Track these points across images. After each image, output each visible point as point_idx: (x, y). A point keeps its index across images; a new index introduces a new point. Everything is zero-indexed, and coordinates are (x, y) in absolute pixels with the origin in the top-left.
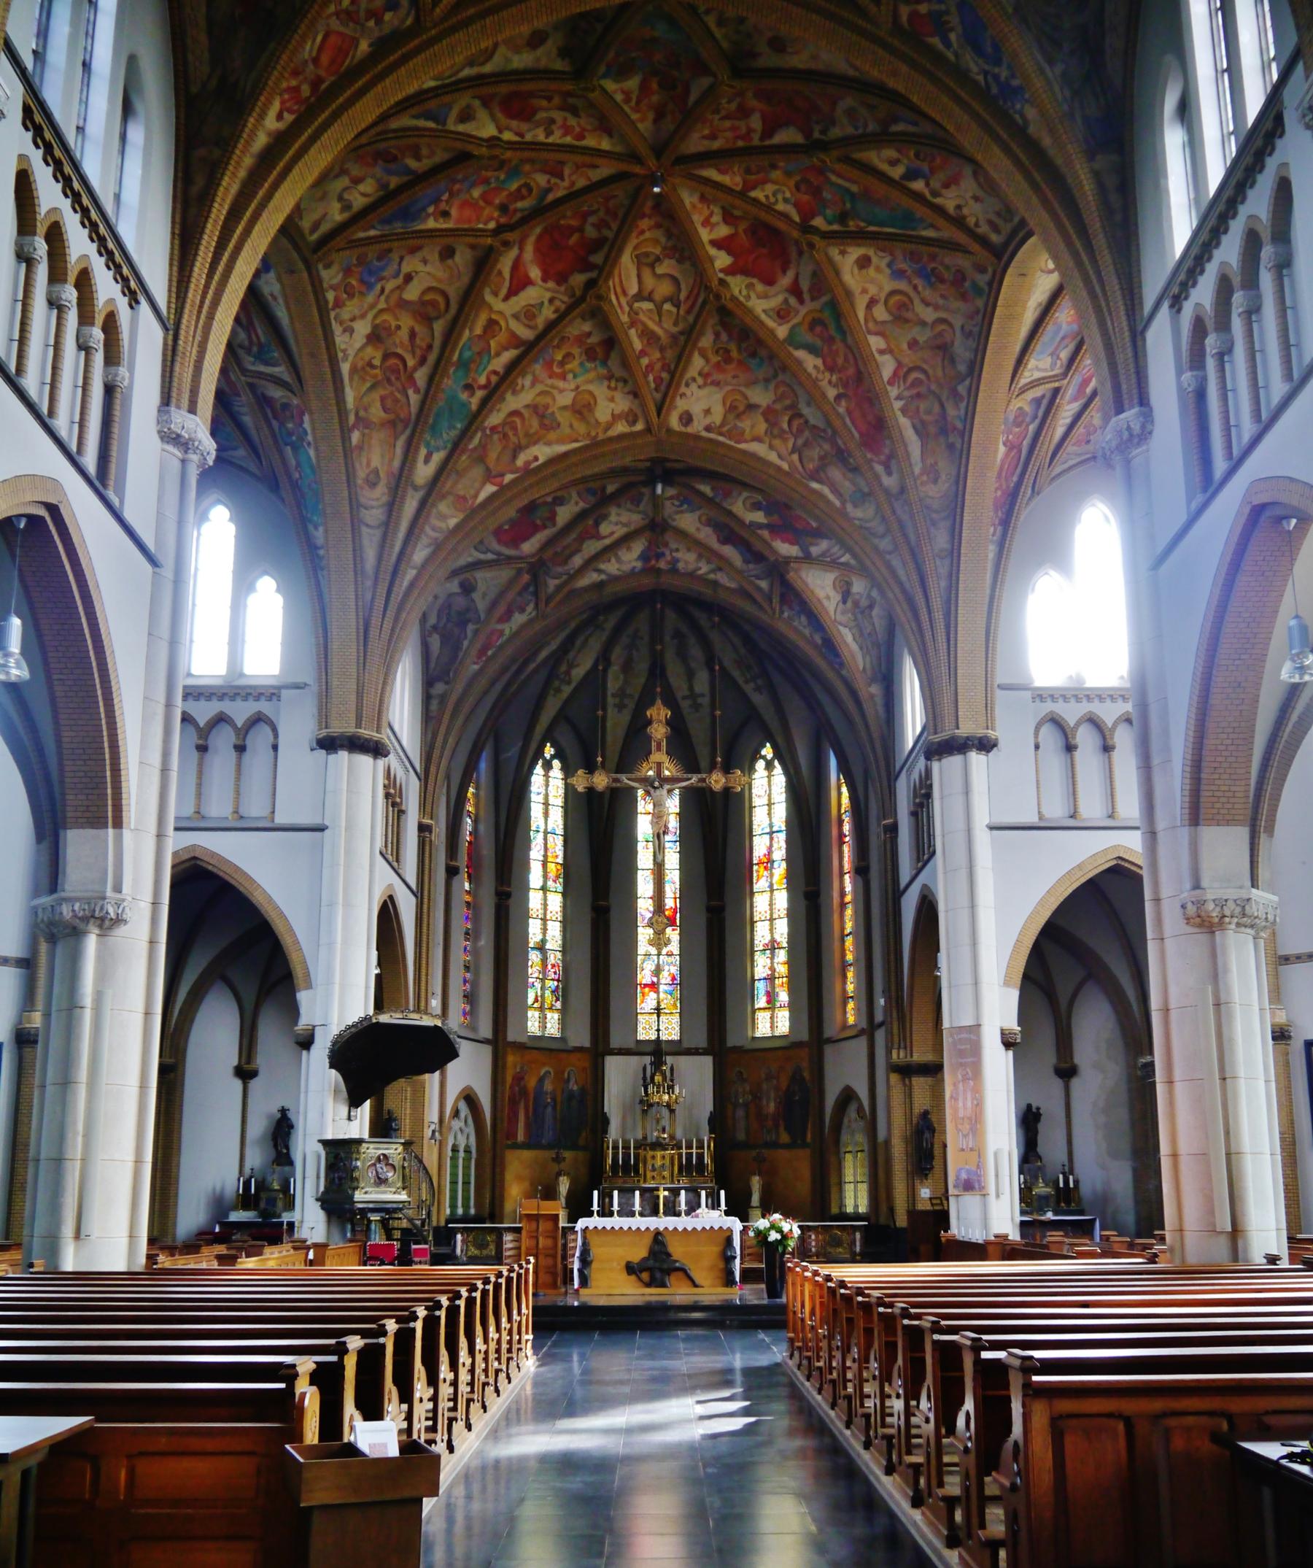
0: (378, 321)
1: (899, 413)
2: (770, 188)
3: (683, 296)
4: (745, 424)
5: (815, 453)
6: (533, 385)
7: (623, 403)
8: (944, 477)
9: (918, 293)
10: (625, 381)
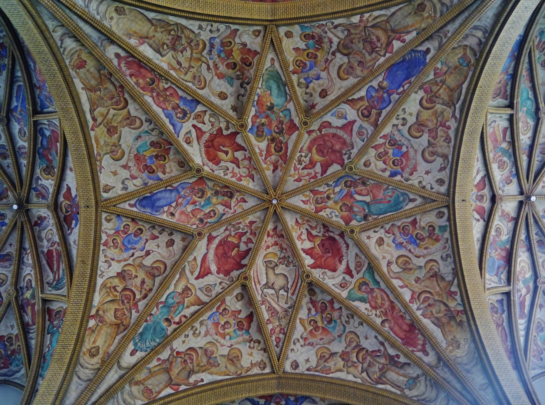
0: (126, 269)
1: (421, 317)
2: (328, 211)
3: (289, 287)
4: (331, 364)
5: (376, 368)
6: (206, 335)
7: (258, 356)
8: (462, 342)
9: (413, 253)
10: (259, 342)
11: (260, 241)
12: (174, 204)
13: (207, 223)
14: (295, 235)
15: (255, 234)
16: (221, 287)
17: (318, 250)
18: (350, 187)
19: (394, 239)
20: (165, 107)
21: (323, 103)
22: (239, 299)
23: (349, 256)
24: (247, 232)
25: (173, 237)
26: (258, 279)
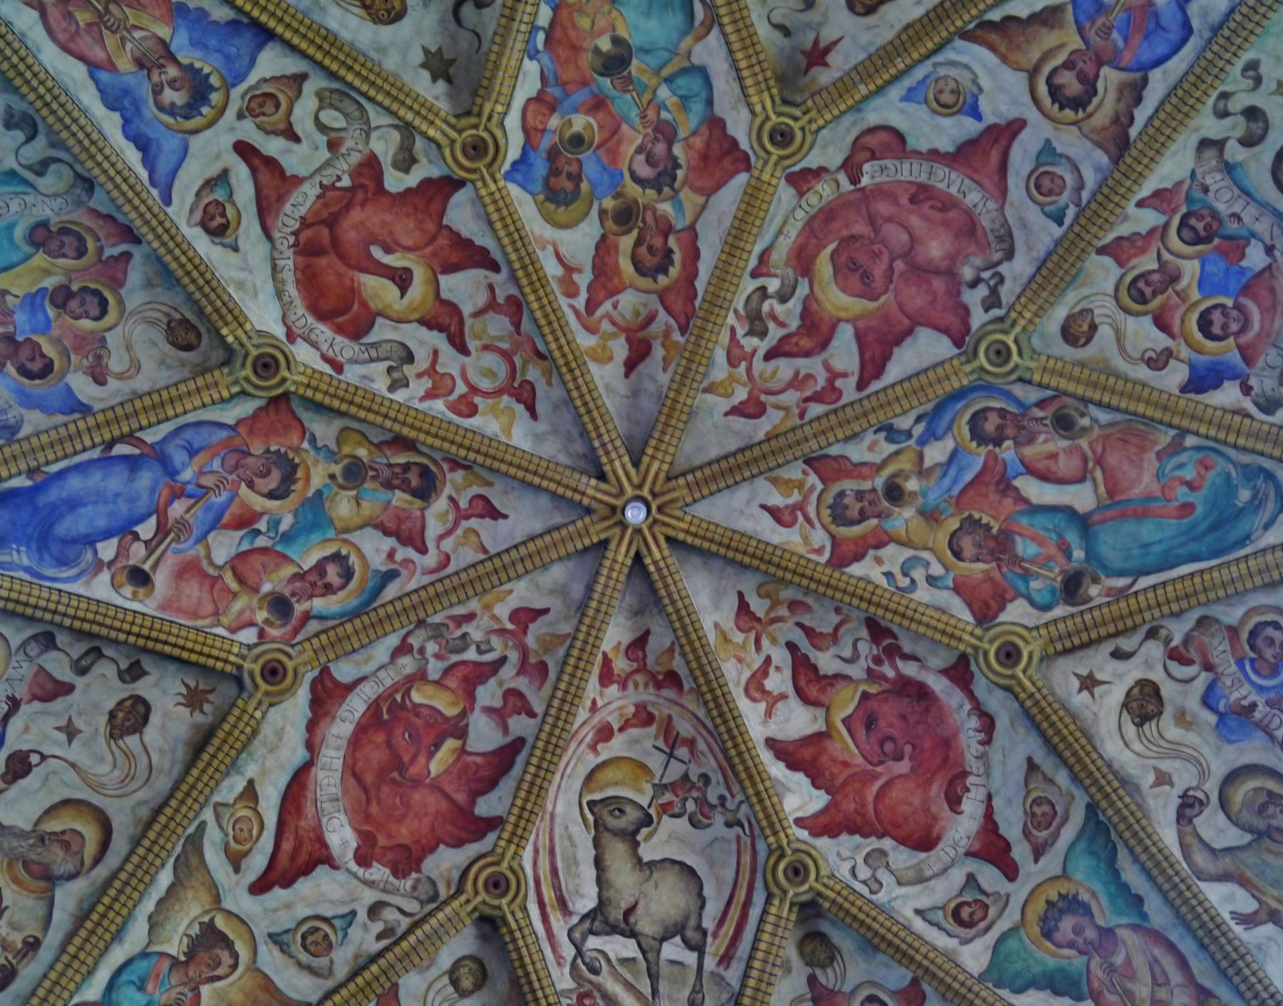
2: (894, 555)
11: (569, 700)
12: (146, 530)
13: (307, 617)
14: (734, 674)
15: (543, 668)
16: (378, 927)
17: (846, 746)
18: (998, 442)
19: (1211, 688)
20: (99, 54)
21: (865, 38)
22: (467, 983)
23: (996, 772)
24: (503, 660)
25: (143, 688)
26: (557, 888)
